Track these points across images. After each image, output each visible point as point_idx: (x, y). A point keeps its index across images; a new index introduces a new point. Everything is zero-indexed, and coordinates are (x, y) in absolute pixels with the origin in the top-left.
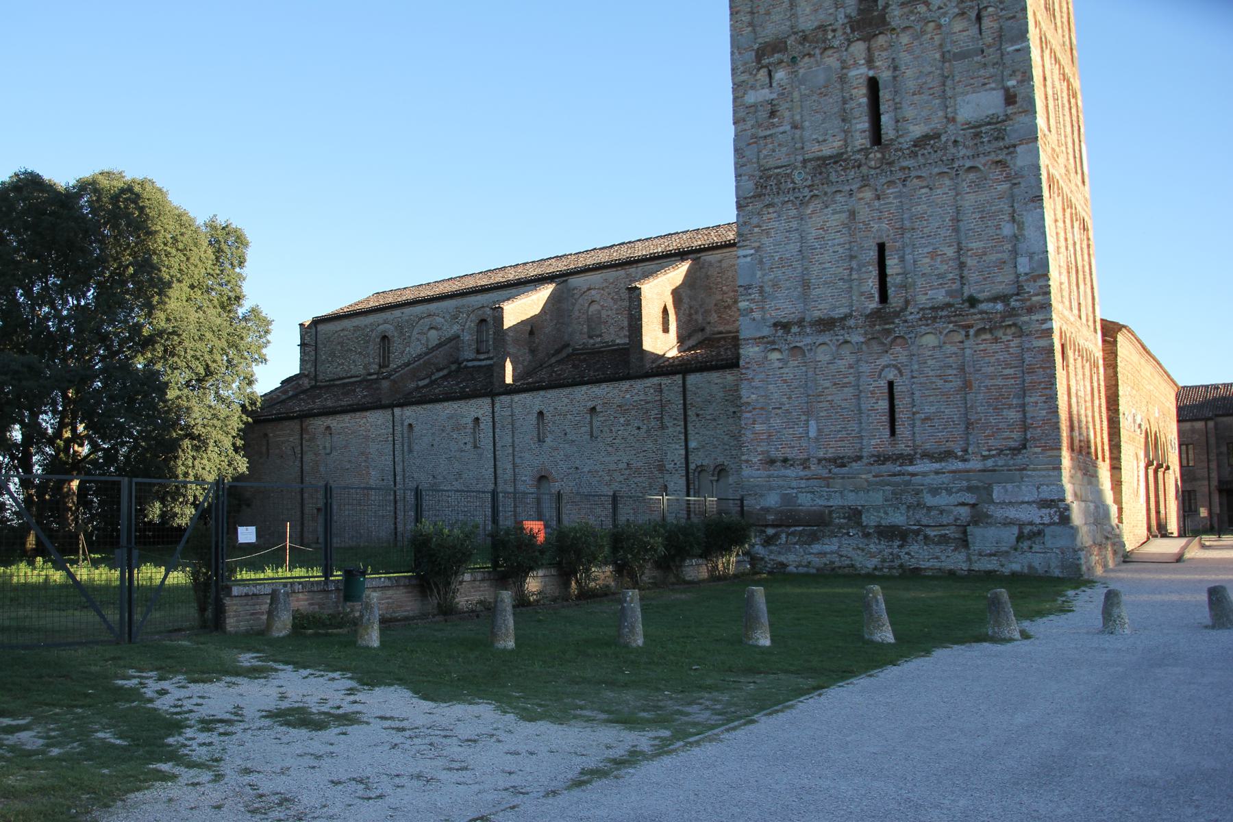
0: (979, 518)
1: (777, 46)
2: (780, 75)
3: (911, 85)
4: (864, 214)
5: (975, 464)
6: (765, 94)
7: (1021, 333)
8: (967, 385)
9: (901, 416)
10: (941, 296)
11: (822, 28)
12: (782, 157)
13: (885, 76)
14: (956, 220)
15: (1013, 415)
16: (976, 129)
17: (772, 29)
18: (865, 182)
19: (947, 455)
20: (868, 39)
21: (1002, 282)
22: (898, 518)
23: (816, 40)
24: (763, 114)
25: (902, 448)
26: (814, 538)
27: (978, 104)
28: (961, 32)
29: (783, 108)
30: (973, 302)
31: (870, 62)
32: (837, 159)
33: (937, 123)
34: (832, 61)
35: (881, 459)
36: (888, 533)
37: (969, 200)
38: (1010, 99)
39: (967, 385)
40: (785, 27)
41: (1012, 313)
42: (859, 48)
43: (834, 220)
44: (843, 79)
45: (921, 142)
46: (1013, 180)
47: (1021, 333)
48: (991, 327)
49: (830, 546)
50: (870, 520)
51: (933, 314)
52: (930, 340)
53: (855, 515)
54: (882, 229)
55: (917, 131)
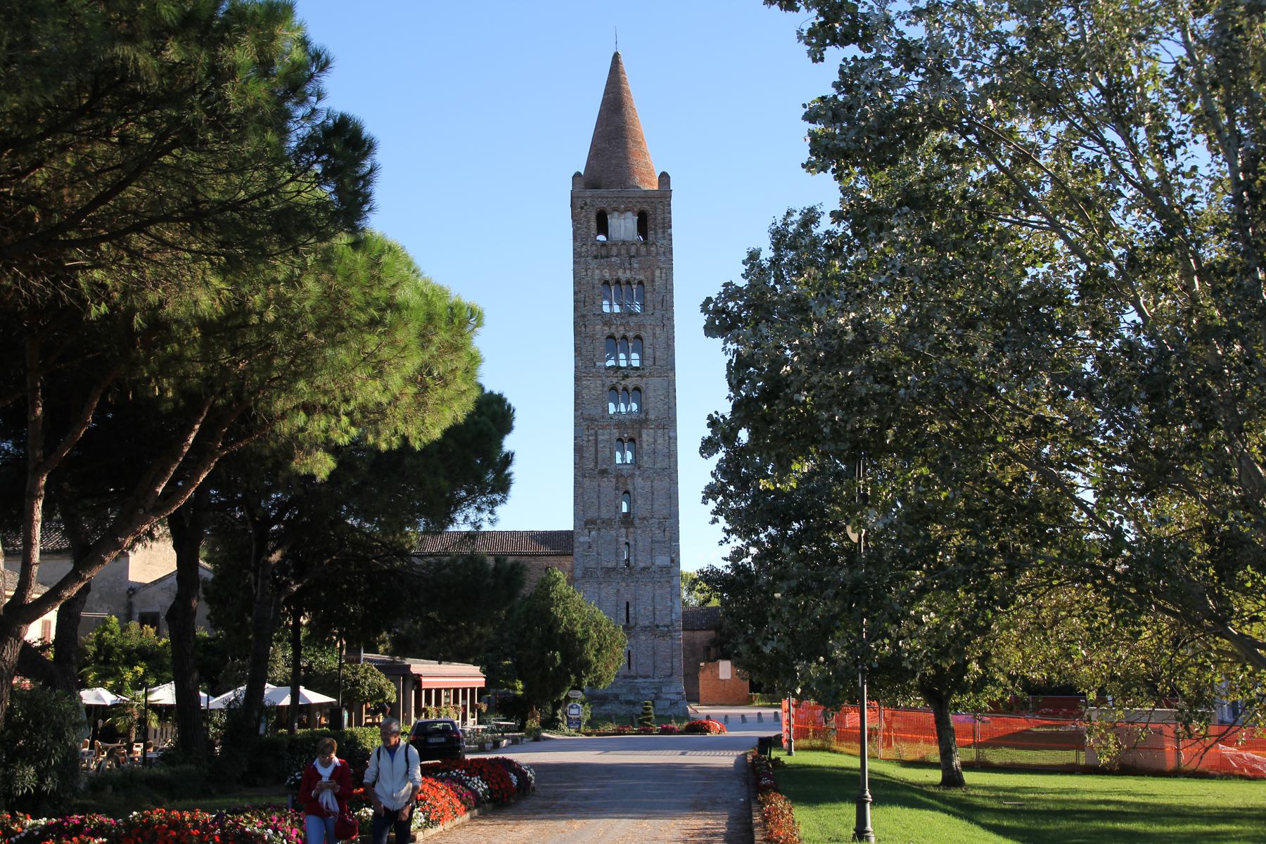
0: (658, 697)
1: (593, 522)
2: (593, 533)
3: (641, 548)
4: (622, 590)
5: (657, 680)
6: (587, 539)
7: (672, 638)
8: (654, 654)
9: (633, 662)
10: (647, 623)
11: (610, 519)
12: (592, 564)
13: (632, 543)
14: (654, 598)
15: (669, 665)
16: (662, 568)
17: (592, 514)
18: (623, 579)
19: (648, 677)
20: (626, 528)
21: (667, 621)
22: (632, 698)
23: (608, 523)
24: (586, 546)
25: (633, 673)
26: (603, 704)
27: (662, 560)
28: (658, 534)
29: (594, 546)
30: (658, 626)
31: (627, 537)
32: (614, 569)
33: (649, 564)
34: (613, 533)
35: (625, 677)
36: (629, 702)
37: (658, 592)
38: (672, 561)
39: (654, 654)
40: (596, 515)
41: (669, 631)
42: (623, 530)
43: (612, 591)
44: (617, 541)
45: (644, 569)
46: (672, 588)
47: (672, 638)
48: (664, 635)
49: (608, 707)
50: (622, 698)
51: (645, 629)
52: (643, 638)
53: (616, 696)
54: (628, 597)
55: (642, 565)
